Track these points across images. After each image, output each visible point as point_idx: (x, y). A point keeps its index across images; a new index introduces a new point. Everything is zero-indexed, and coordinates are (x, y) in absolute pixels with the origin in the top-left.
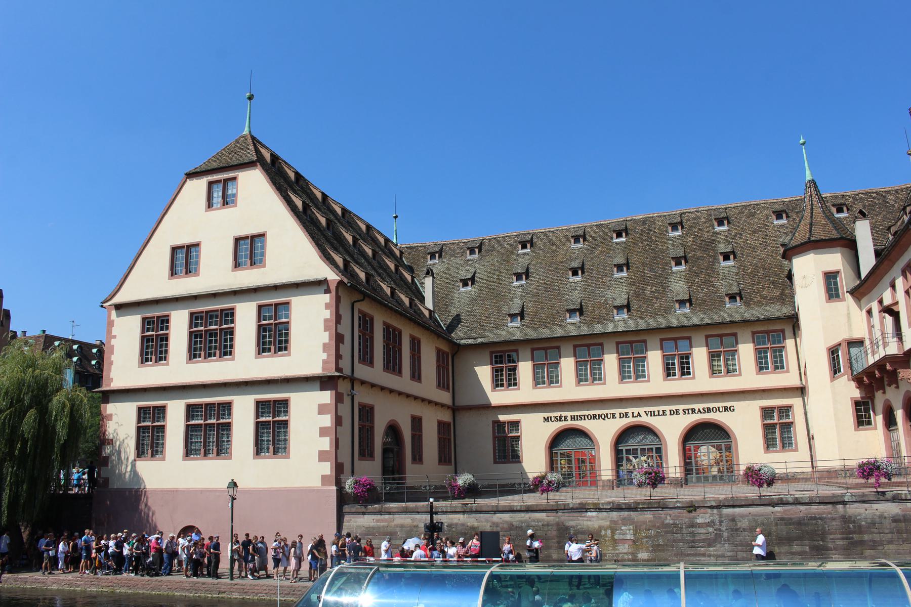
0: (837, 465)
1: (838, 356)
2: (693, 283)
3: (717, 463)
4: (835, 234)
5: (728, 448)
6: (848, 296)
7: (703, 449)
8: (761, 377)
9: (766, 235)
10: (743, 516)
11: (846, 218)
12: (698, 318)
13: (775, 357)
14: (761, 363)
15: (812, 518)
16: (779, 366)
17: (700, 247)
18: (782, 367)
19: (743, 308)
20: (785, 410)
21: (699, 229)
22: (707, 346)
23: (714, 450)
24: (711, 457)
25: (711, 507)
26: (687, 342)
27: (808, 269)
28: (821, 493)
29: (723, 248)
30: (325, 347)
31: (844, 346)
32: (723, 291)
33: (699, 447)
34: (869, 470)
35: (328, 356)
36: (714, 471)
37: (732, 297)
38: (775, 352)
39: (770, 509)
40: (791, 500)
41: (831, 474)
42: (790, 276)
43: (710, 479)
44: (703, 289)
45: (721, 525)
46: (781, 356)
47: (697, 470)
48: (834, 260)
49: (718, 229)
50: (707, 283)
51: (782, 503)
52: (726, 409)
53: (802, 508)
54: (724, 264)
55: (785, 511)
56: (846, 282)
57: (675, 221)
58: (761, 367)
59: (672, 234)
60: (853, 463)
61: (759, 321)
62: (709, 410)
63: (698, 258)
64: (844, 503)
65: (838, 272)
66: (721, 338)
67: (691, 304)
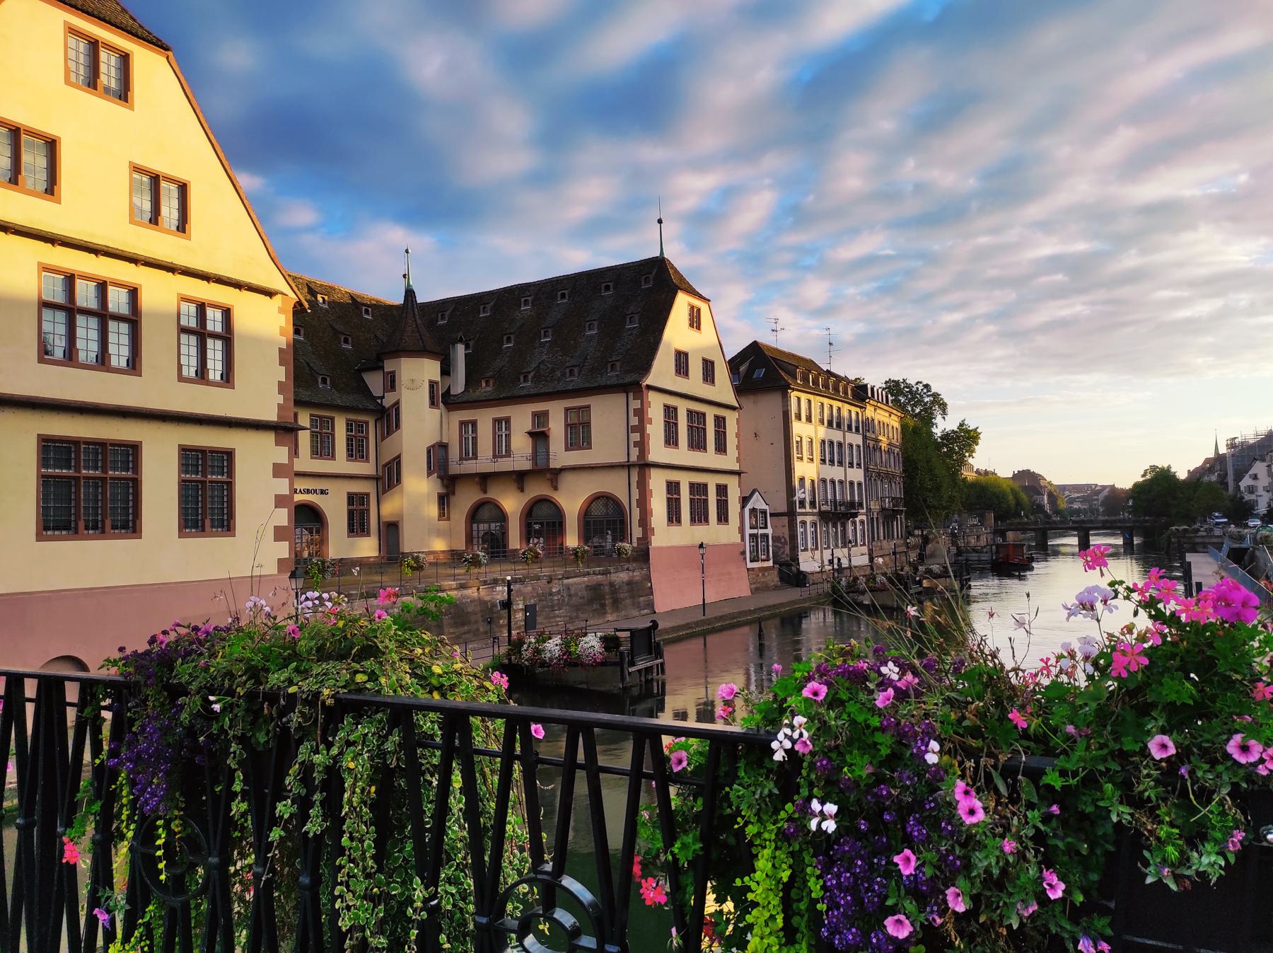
30: (282, 388)
35: (285, 399)
52: (323, 492)
62: (308, 491)
65: (437, 383)
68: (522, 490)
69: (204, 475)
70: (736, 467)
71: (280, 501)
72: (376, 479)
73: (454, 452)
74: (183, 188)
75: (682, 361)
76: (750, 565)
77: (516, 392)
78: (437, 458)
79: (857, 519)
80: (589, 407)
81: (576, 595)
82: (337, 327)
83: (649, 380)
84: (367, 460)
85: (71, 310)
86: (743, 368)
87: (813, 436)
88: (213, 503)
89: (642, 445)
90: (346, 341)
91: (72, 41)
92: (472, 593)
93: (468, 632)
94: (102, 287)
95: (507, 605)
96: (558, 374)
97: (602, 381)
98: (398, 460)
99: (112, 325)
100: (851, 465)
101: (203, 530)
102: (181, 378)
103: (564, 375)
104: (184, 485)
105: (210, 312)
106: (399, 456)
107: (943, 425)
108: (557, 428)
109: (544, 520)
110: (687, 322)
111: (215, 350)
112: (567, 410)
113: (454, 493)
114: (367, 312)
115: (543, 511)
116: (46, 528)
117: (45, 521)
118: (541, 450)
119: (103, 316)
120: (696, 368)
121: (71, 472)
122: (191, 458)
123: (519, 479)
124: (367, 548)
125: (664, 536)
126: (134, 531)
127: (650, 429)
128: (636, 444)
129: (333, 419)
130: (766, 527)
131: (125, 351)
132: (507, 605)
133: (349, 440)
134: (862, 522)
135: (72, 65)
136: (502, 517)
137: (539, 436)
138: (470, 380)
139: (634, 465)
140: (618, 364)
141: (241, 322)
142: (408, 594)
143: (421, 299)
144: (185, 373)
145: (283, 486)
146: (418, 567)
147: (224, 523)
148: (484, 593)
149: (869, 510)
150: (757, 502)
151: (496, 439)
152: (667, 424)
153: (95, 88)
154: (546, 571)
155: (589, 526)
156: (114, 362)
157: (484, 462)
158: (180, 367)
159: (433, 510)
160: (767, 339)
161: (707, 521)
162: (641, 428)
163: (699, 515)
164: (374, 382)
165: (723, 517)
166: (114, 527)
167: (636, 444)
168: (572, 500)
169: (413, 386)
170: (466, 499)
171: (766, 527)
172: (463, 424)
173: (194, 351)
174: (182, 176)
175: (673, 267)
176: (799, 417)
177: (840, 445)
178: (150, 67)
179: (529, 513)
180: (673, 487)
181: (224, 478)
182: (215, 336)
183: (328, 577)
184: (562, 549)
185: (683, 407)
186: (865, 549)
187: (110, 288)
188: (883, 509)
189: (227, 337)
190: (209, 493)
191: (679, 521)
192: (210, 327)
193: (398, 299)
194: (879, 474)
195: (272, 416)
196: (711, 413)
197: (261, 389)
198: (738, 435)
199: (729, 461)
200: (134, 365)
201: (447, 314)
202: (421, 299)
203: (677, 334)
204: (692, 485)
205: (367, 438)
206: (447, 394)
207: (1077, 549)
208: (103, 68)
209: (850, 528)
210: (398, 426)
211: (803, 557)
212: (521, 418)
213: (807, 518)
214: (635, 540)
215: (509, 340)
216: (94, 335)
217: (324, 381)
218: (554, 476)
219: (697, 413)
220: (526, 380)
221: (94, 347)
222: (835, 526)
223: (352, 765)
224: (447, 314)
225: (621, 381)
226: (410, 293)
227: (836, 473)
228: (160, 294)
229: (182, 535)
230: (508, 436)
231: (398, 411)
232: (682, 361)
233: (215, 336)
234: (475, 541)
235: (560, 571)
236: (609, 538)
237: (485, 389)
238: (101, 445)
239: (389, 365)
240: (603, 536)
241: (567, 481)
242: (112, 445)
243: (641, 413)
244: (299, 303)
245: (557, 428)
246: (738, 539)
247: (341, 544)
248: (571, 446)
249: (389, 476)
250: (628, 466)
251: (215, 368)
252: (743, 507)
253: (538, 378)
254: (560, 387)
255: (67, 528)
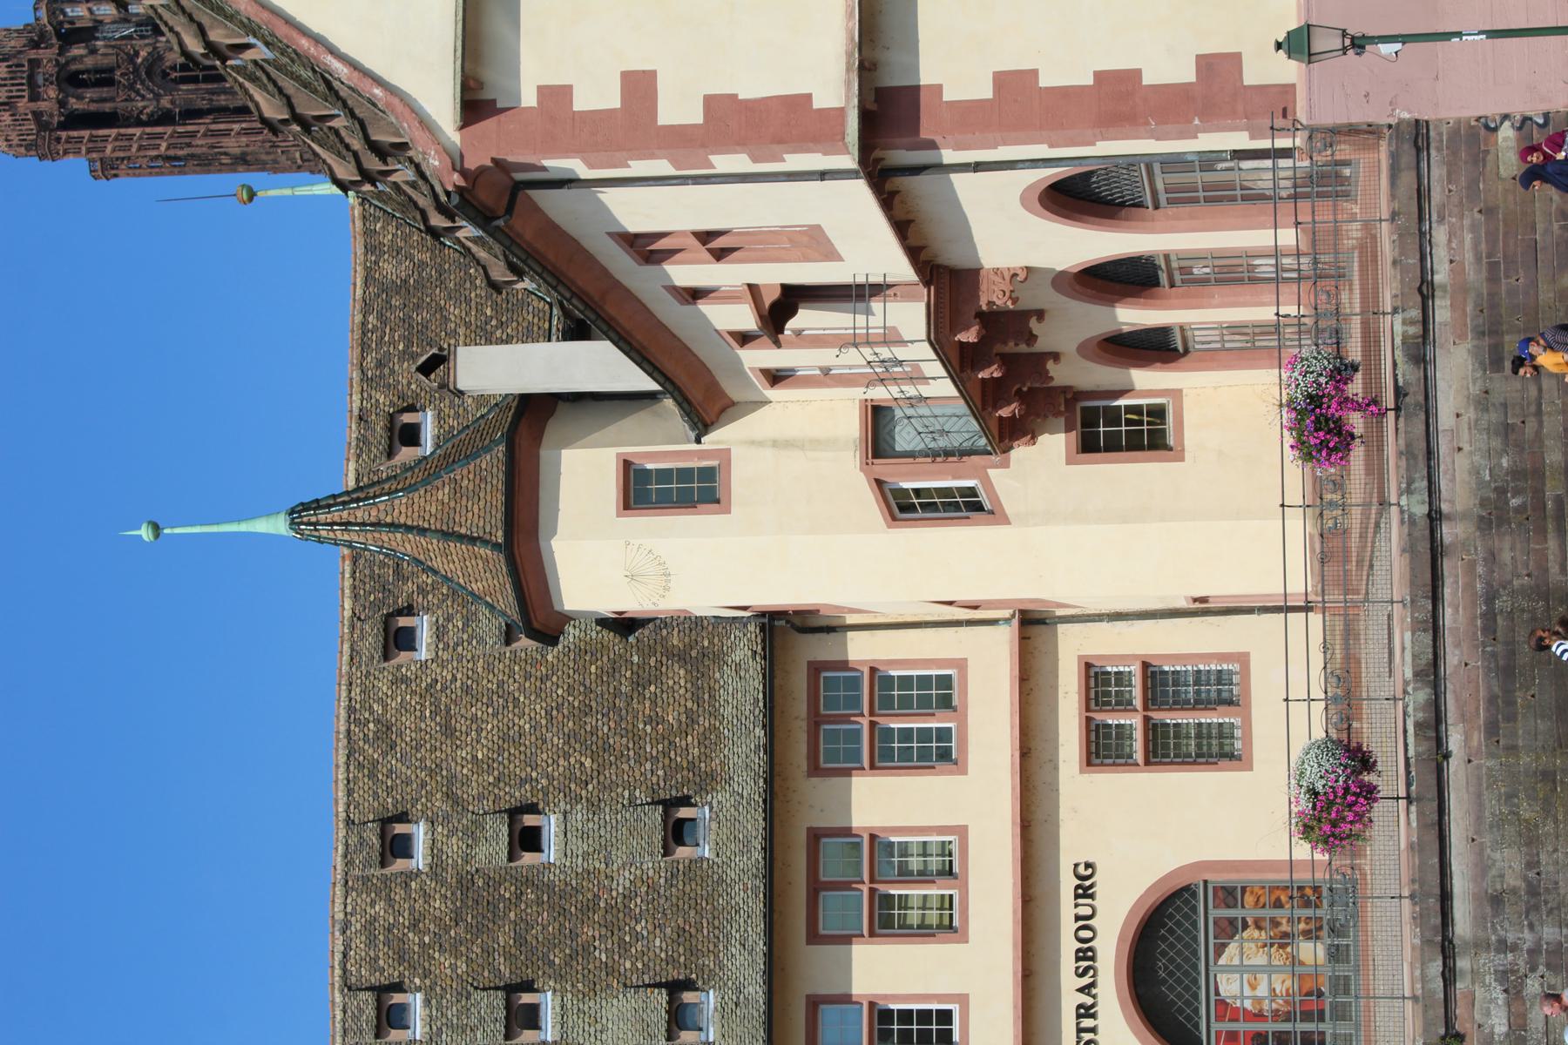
0: (1298, 526)
1: (917, 492)
2: (610, 970)
3: (1284, 941)
4: (492, 461)
5: (1229, 895)
6: (712, 440)
7: (1229, 986)
8: (975, 757)
9: (467, 690)
10: (1482, 868)
11: (440, 418)
12: (744, 965)
13: (906, 702)
14: (924, 755)
15: (1489, 628)
16: (940, 692)
17: (478, 930)
18: (945, 682)
19: (721, 797)
20: (1100, 684)
21: (414, 926)
22: (847, 940)
23: (1232, 948)
24: (1260, 959)
25: (1449, 976)
26: (828, 1013)
27: (602, 559)
28: (1400, 590)
29: (493, 847)
31: (884, 468)
32: (652, 864)
33: (1222, 1003)
34: (1320, 427)
36: (1311, 952)
37: (677, 833)
38: (887, 702)
39: (1456, 768)
40: (1423, 695)
41: (1333, 552)
42: (624, 625)
43: (1342, 970)
44: (637, 937)
45: (1514, 948)
46: (906, 682)
47: (1307, 1016)
48: (582, 473)
49: (420, 859)
50: (616, 917)
51: (1434, 725)
53: (1452, 658)
54: (552, 851)
55: (1463, 718)
56: (663, 442)
57: (370, 1011)
58: (939, 753)
59: (419, 1029)
60: (1296, 475)
61: (771, 749)
62: (1086, 954)
63: (520, 941)
64: (1435, 517)
66: (820, 886)
67: (689, 985)
68: (1040, 314)
81: (1530, 839)
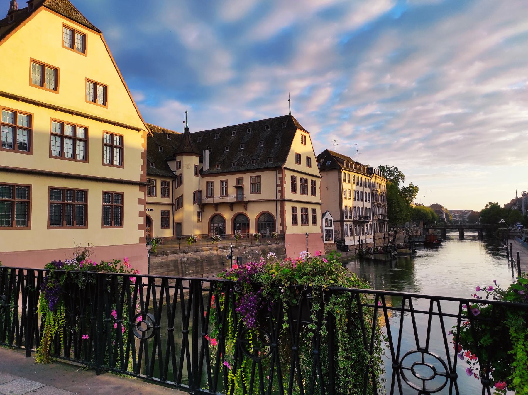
52: (151, 210)
65: (198, 166)
69: (112, 203)
70: (320, 202)
71: (141, 214)
72: (172, 205)
73: (204, 194)
74: (105, 88)
75: (298, 157)
76: (325, 242)
77: (230, 170)
78: (197, 197)
79: (369, 224)
80: (260, 176)
82: (157, 143)
83: (285, 166)
84: (169, 197)
85: (62, 137)
86: (322, 161)
87: (351, 189)
88: (115, 214)
89: (282, 192)
90: (161, 149)
91: (65, 30)
92: (215, 252)
93: (213, 268)
94: (74, 127)
95: (230, 257)
96: (247, 162)
97: (265, 166)
98: (181, 197)
99: (78, 143)
100: (366, 201)
101: (111, 225)
102: (104, 164)
103: (250, 163)
104: (104, 207)
105: (115, 137)
106: (182, 196)
107: (403, 185)
108: (247, 185)
109: (240, 222)
110: (300, 142)
111: (117, 152)
112: (251, 177)
113: (204, 211)
114: (169, 137)
115: (241, 219)
116: (51, 224)
117: (51, 221)
118: (240, 194)
119: (74, 139)
120: (304, 160)
121: (61, 202)
122: (107, 196)
123: (231, 205)
124: (168, 233)
125: (291, 230)
126: (85, 226)
127: (285, 185)
128: (280, 192)
129: (156, 180)
130: (332, 226)
131: (82, 153)
132: (230, 257)
133: (162, 189)
134: (370, 225)
135: (64, 39)
136: (224, 221)
137: (239, 188)
138: (211, 165)
139: (279, 200)
140: (272, 159)
141: (127, 142)
142: (190, 252)
143: (191, 131)
144: (105, 162)
145: (142, 208)
146: (194, 241)
147: (120, 223)
148: (219, 252)
149: (373, 220)
150: (328, 216)
151: (222, 189)
152: (292, 183)
153: (73, 48)
154: (244, 244)
155: (260, 226)
156: (78, 157)
157: (217, 198)
158: (103, 159)
159: (195, 218)
160: (331, 149)
161: (308, 223)
162: (281, 185)
163: (305, 221)
164: (172, 165)
165: (314, 222)
166: (77, 224)
167: (280, 192)
168: (253, 215)
169: (188, 167)
170: (209, 214)
171: (332, 226)
172: (208, 183)
173: (108, 153)
174: (106, 83)
175: (295, 119)
176: (345, 181)
177: (362, 192)
178: (93, 38)
179: (235, 220)
180: (294, 210)
181: (120, 204)
182: (117, 147)
183: (159, 245)
184: (248, 235)
185: (299, 176)
186: (372, 236)
187: (77, 128)
188: (379, 220)
189: (121, 148)
190: (114, 210)
191: (297, 223)
192: (115, 143)
193: (181, 131)
194: (377, 205)
195: (138, 179)
196: (310, 179)
197: (134, 169)
198: (320, 188)
199: (317, 199)
200: (86, 158)
201: (201, 138)
202: (191, 131)
203: (296, 146)
204: (302, 209)
205: (169, 188)
206: (201, 170)
207: (477, 238)
208: (76, 41)
209: (366, 227)
210: (182, 183)
211: (346, 239)
212: (232, 180)
213: (348, 223)
214: (279, 231)
215: (227, 149)
216: (70, 146)
217: (152, 165)
218: (245, 204)
219: (304, 179)
220: (234, 165)
221: (70, 151)
222: (359, 226)
223: (338, 311)
224: (201, 138)
225: (274, 166)
226: (187, 129)
227: (360, 204)
228: (97, 130)
229: (103, 227)
230: (227, 188)
231: (182, 177)
232: (298, 157)
233: (117, 147)
234: (212, 231)
235: (249, 244)
236: (268, 230)
237: (217, 169)
238: (73, 191)
239: (178, 159)
240: (265, 230)
241: (251, 206)
242: (77, 191)
243: (282, 179)
244: (149, 134)
245: (247, 185)
246: (320, 232)
247: (158, 232)
248: (253, 192)
249: (178, 204)
250: (277, 201)
251: (116, 162)
252: (322, 218)
253: (239, 165)
254: (248, 168)
255: (59, 224)
